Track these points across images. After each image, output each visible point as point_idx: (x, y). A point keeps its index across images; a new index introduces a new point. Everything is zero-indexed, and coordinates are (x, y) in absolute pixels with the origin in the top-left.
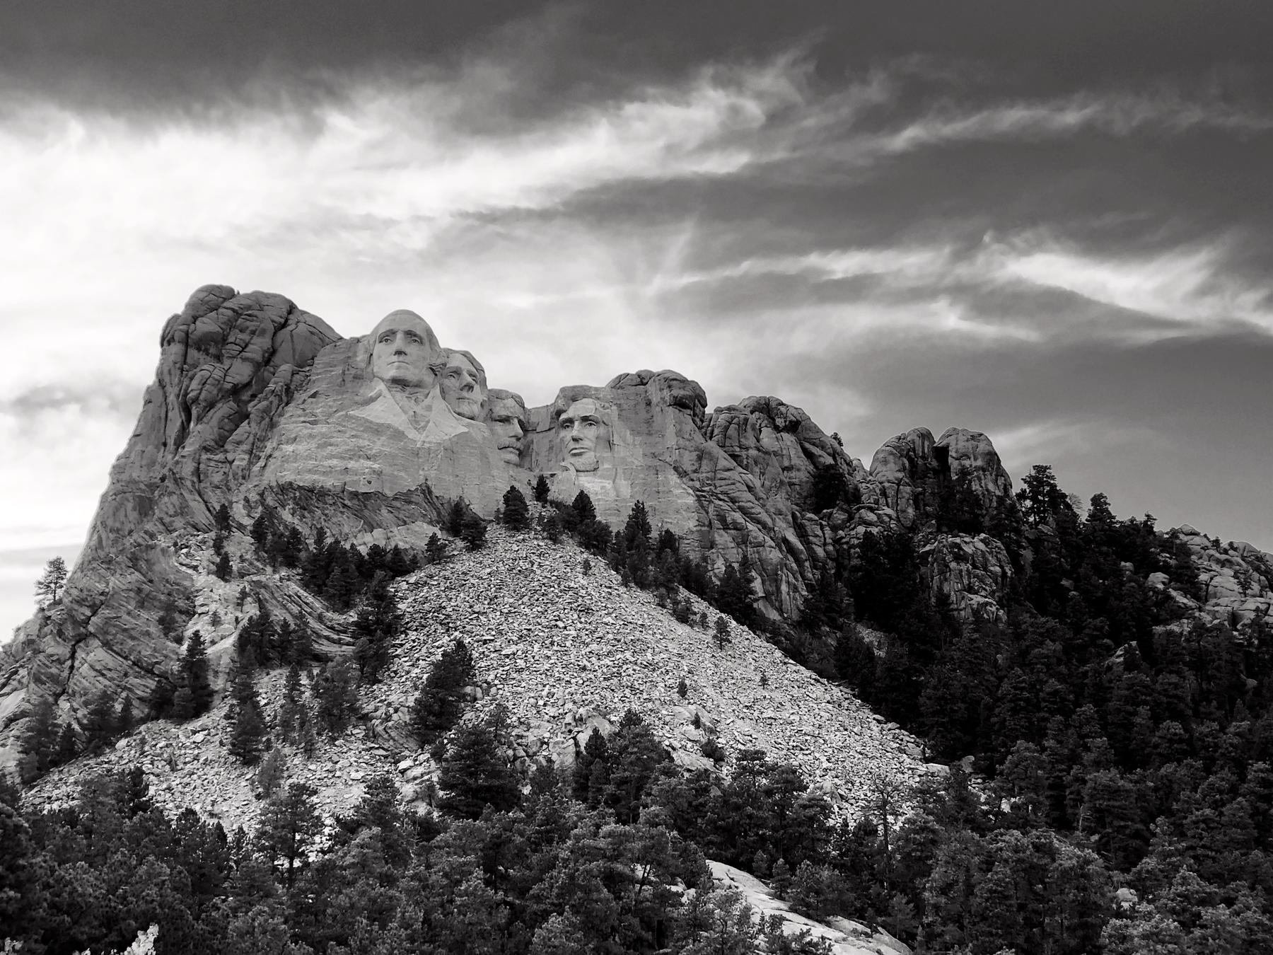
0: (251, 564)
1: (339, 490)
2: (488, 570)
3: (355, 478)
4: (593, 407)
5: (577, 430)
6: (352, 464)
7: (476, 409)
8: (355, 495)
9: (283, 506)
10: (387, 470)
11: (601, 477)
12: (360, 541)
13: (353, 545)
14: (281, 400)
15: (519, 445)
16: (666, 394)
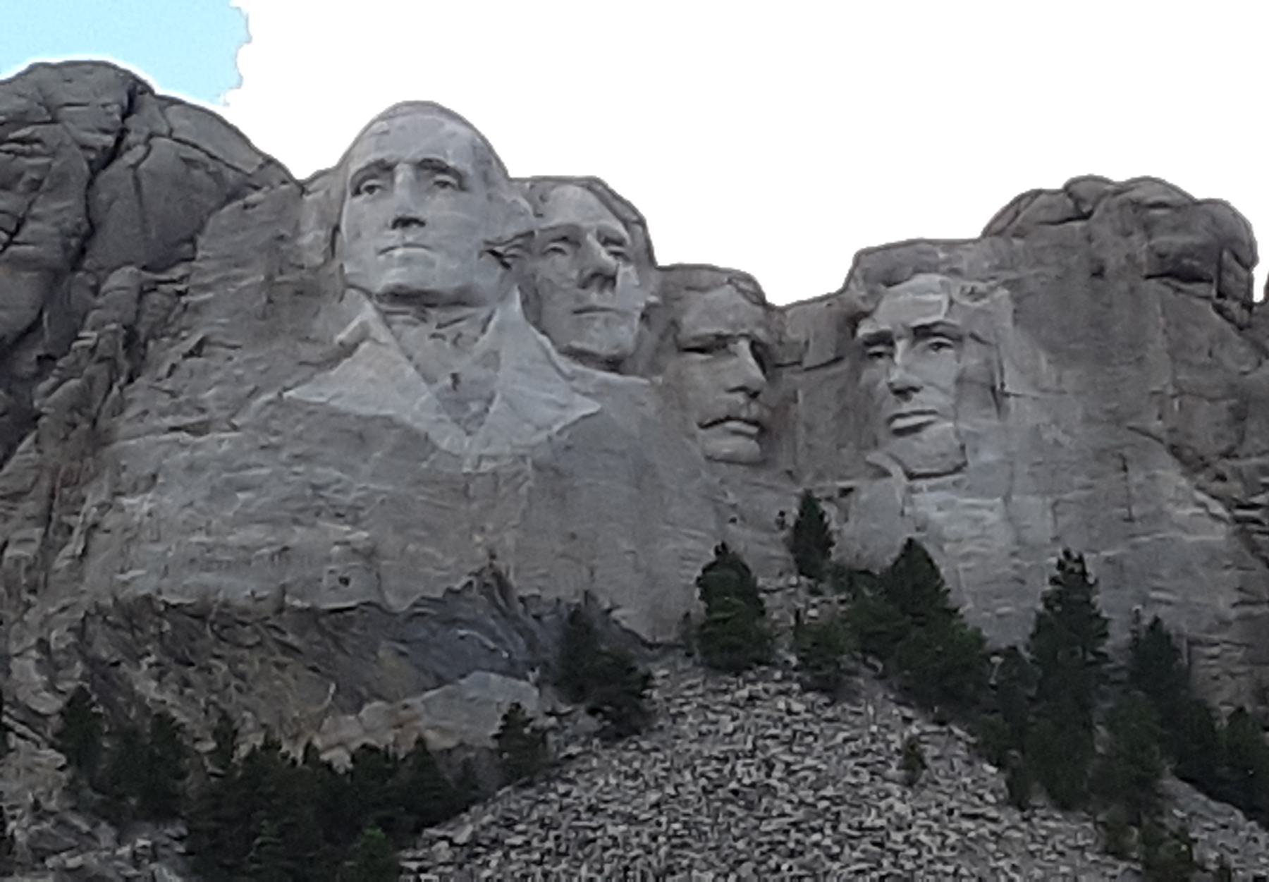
0: (61, 823)
1: (267, 608)
2: (653, 797)
3: (309, 573)
4: (943, 298)
5: (903, 364)
6: (298, 536)
7: (626, 335)
8: (312, 615)
9: (137, 659)
10: (391, 542)
11: (970, 491)
12: (333, 738)
13: (309, 747)
14: (115, 368)
15: (754, 410)
16: (1139, 245)
